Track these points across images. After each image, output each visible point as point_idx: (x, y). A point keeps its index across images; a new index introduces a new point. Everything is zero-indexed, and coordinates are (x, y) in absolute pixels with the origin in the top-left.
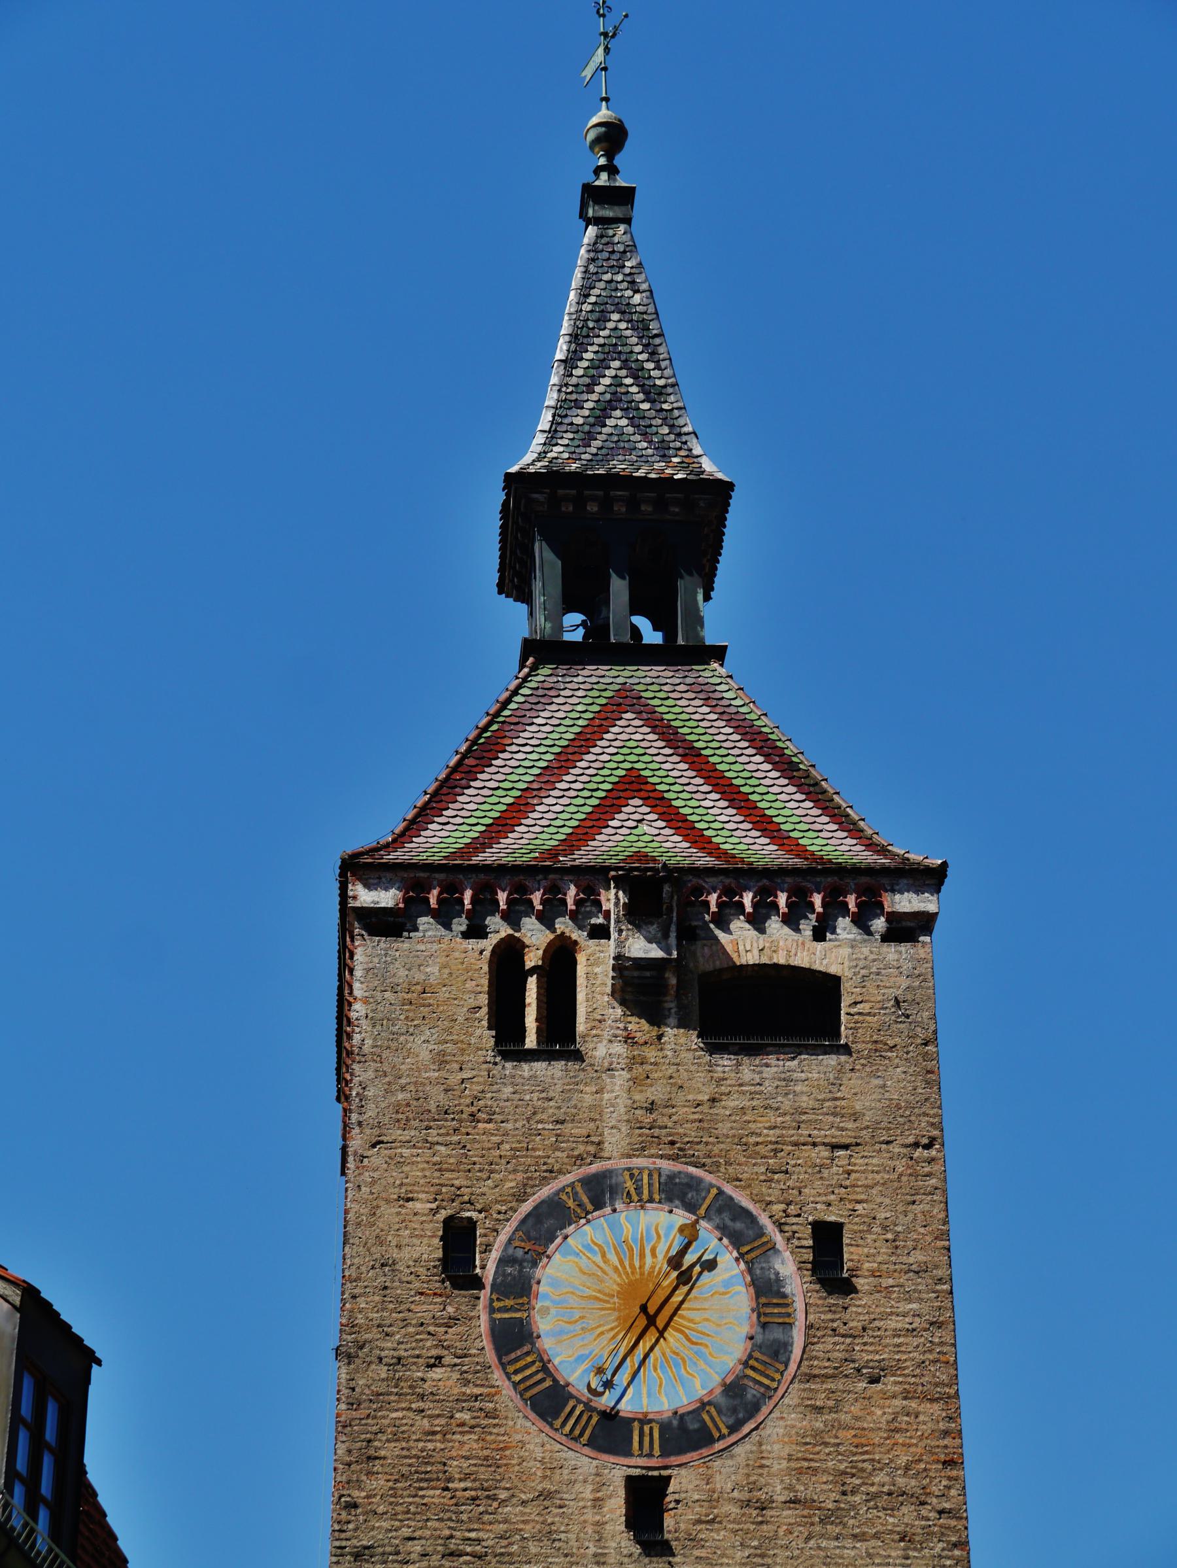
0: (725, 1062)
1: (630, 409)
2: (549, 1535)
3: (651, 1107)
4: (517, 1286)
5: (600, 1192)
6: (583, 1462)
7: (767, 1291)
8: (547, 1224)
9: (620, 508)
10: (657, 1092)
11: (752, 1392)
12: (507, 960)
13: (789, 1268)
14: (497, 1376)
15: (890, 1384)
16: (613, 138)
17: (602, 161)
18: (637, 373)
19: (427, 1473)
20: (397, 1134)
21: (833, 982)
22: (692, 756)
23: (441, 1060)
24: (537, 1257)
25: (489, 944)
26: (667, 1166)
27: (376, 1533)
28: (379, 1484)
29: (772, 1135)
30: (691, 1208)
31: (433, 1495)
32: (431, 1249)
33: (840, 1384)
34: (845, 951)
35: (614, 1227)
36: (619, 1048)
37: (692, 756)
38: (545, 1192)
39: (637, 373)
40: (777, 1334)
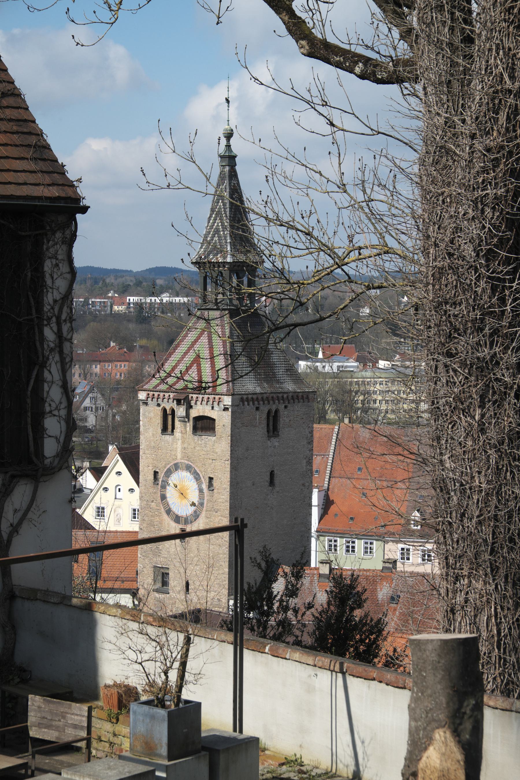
0: (196, 438)
5: (177, 467)
7: (201, 491)
8: (169, 473)
10: (186, 445)
11: (198, 513)
12: (165, 410)
13: (205, 486)
15: (219, 513)
20: (147, 452)
21: (214, 420)
23: (153, 435)
25: (160, 408)
26: (186, 462)
29: (203, 456)
30: (190, 472)
31: (152, 528)
32: (151, 477)
33: (211, 513)
34: (216, 413)
35: (179, 476)
36: (180, 434)
38: (168, 466)
40: (202, 501)
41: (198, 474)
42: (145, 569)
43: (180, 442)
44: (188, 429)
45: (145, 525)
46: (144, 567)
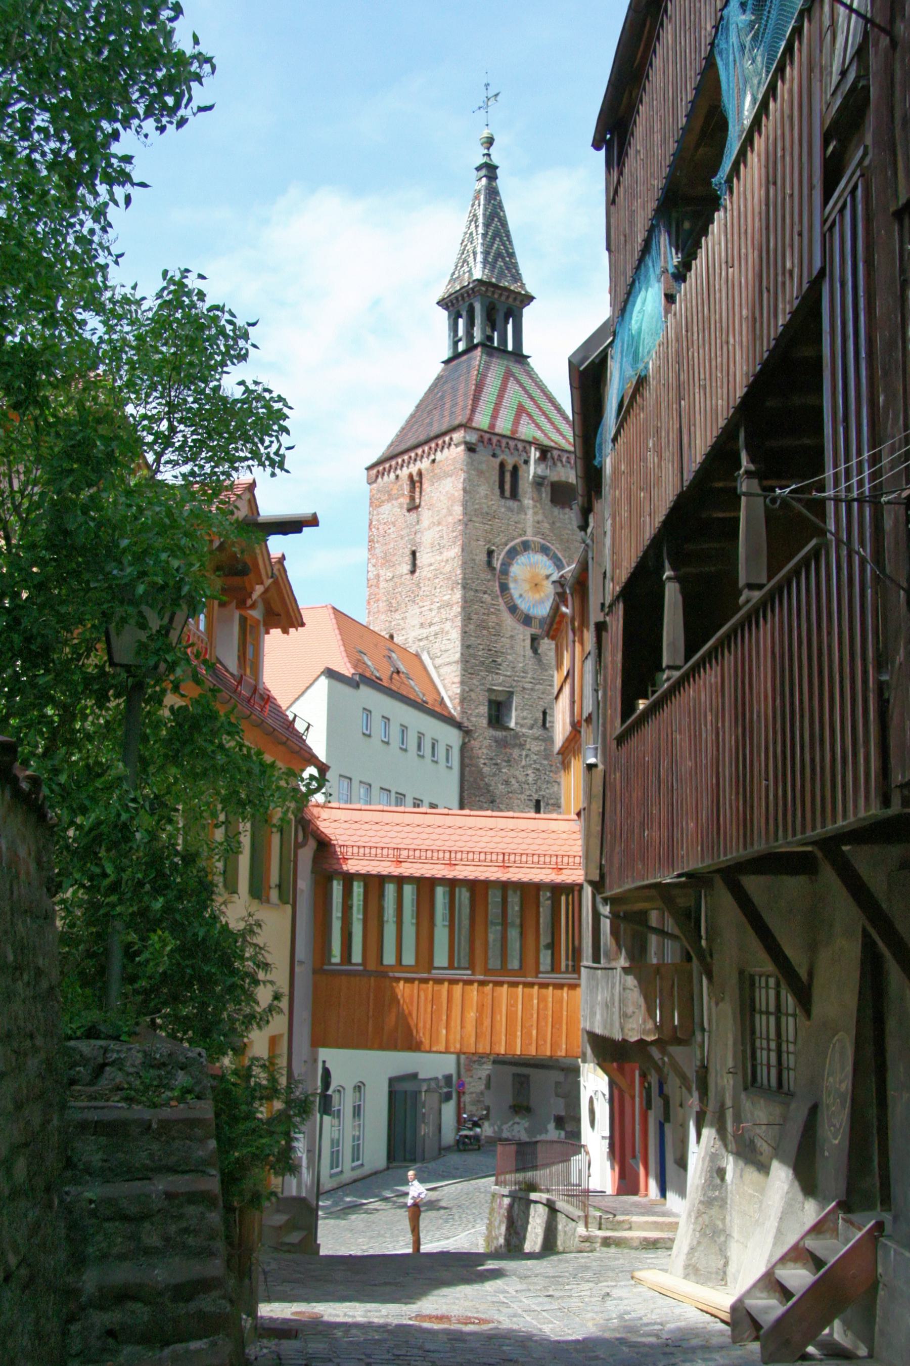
0: (556, 511)
1: (503, 259)
2: (512, 647)
3: (538, 522)
4: (505, 572)
5: (526, 546)
6: (520, 628)
8: (513, 553)
9: (503, 298)
12: (502, 465)
14: (500, 600)
16: (490, 142)
17: (486, 151)
18: (504, 244)
19: (483, 626)
22: (532, 399)
24: (510, 564)
27: (472, 641)
28: (472, 627)
30: (547, 555)
31: (485, 632)
32: (483, 557)
36: (531, 502)
37: (532, 399)
38: (511, 544)
39: (504, 244)
41: (559, 560)
42: (473, 695)
43: (530, 512)
44: (544, 495)
45: (472, 627)
46: (471, 690)
